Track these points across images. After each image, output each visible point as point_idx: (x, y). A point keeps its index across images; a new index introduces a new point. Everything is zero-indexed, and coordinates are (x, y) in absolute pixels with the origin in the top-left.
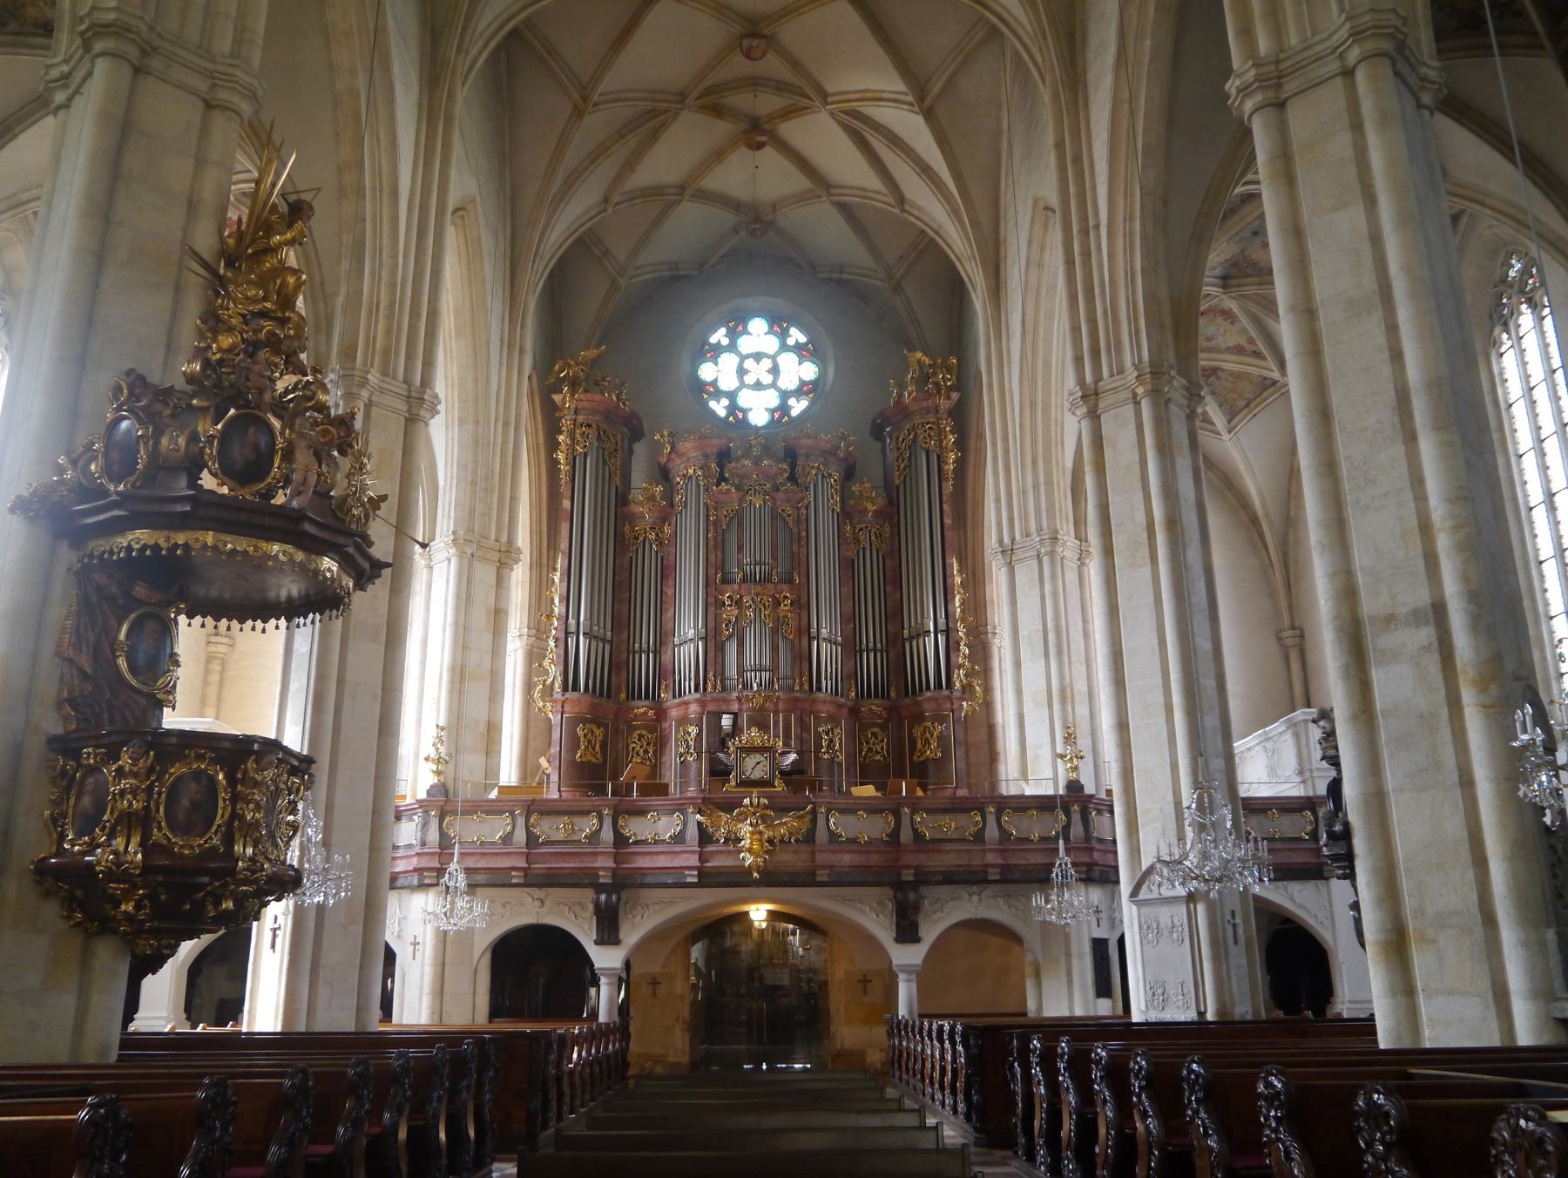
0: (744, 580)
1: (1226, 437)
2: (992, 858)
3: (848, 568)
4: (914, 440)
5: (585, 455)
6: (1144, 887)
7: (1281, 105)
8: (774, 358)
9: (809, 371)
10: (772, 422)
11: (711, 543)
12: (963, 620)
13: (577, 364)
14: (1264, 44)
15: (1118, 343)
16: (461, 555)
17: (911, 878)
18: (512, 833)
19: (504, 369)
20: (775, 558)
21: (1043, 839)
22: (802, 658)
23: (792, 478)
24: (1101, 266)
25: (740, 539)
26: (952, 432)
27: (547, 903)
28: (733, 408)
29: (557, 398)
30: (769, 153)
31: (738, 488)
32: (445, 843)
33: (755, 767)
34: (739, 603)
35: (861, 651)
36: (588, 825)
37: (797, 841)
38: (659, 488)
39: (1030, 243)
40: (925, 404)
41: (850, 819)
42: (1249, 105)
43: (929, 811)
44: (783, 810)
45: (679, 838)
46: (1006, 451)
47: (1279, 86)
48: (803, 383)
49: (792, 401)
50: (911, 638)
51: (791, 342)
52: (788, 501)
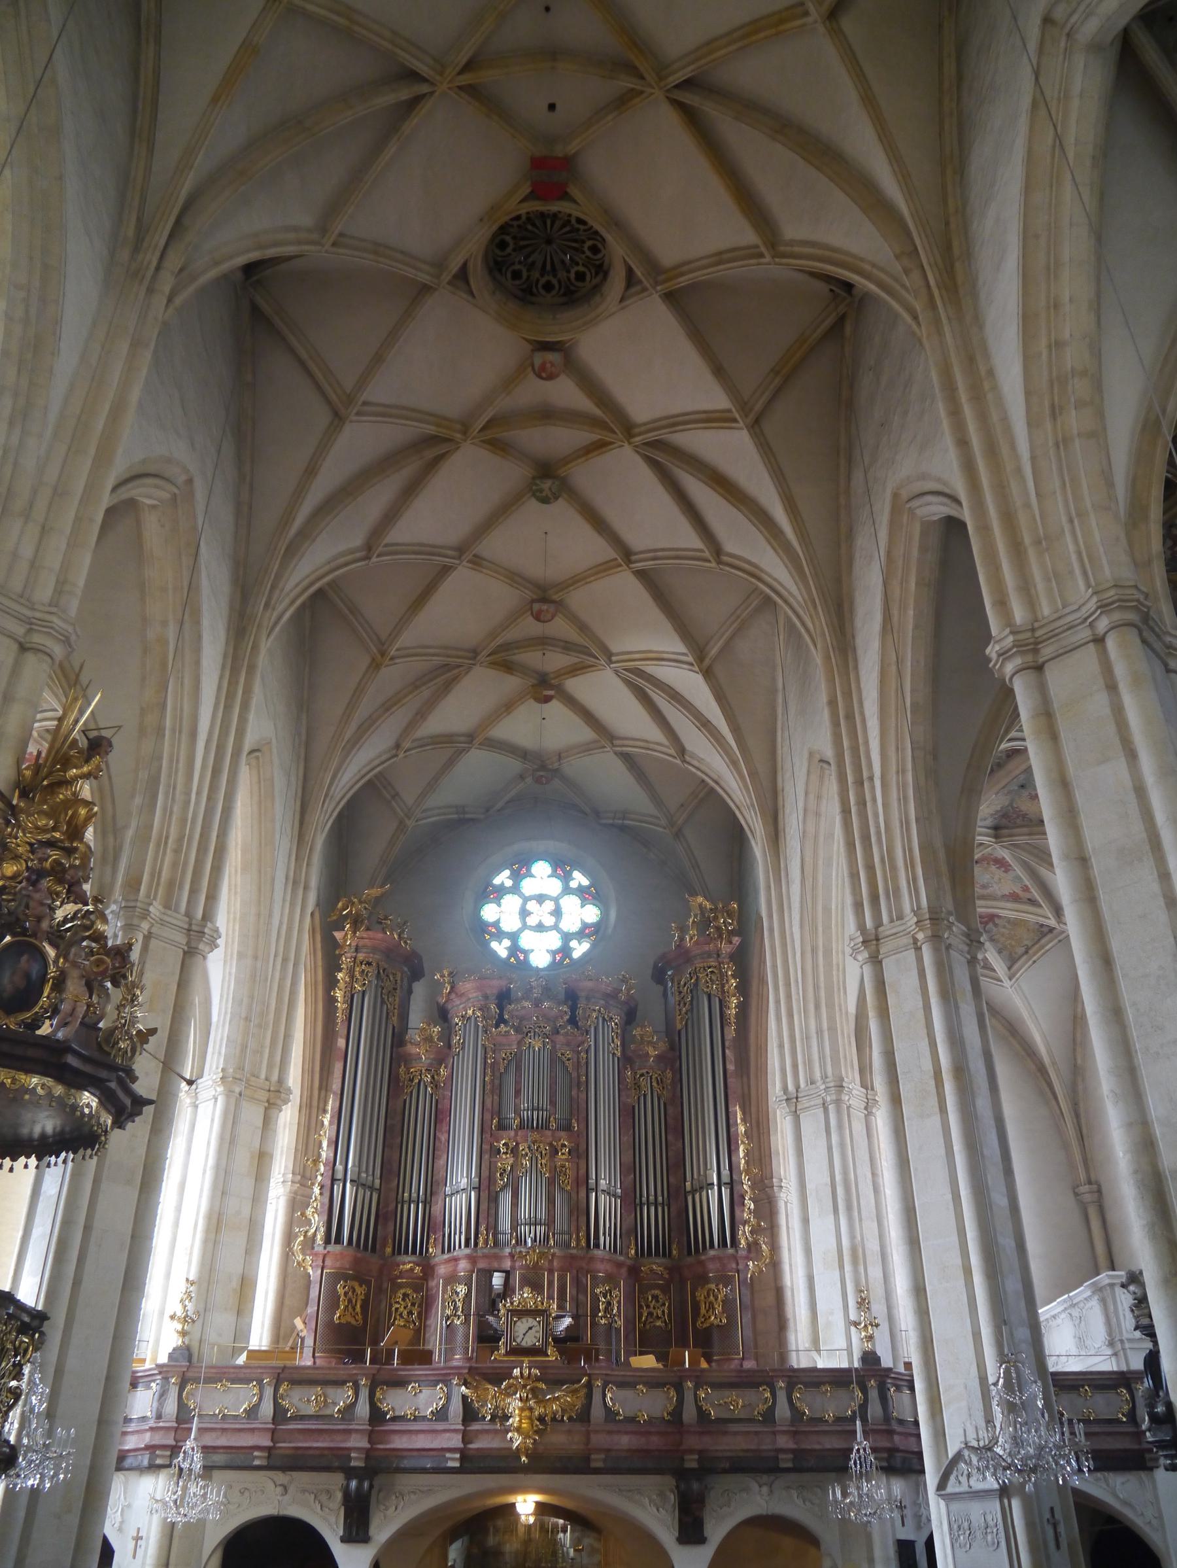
0: (521, 1127)
1: (1007, 983)
2: (783, 1442)
3: (628, 1115)
4: (696, 984)
5: (364, 993)
6: (952, 1478)
7: (1039, 668)
8: (556, 900)
9: (592, 914)
10: (554, 965)
11: (488, 1087)
12: (747, 1172)
13: (360, 902)
14: (1019, 615)
15: (897, 890)
16: (229, 1093)
17: (694, 1465)
18: (257, 1405)
19: (287, 905)
20: (553, 1103)
21: (839, 1420)
22: (580, 1212)
23: (573, 1021)
24: (876, 815)
25: (518, 1083)
26: (733, 976)
27: (291, 1490)
28: (515, 949)
29: (338, 935)
30: (556, 706)
31: (518, 1030)
32: (183, 1416)
33: (527, 1332)
34: (514, 1151)
35: (641, 1204)
36: (342, 1397)
37: (570, 1419)
38: (437, 1029)
39: (806, 794)
40: (706, 948)
41: (628, 1393)
42: (1009, 668)
43: (714, 1386)
44: (555, 1383)
45: (441, 1414)
46: (789, 997)
47: (1036, 651)
48: (585, 926)
49: (574, 944)
50: (693, 1191)
51: (573, 884)
52: (568, 1044)
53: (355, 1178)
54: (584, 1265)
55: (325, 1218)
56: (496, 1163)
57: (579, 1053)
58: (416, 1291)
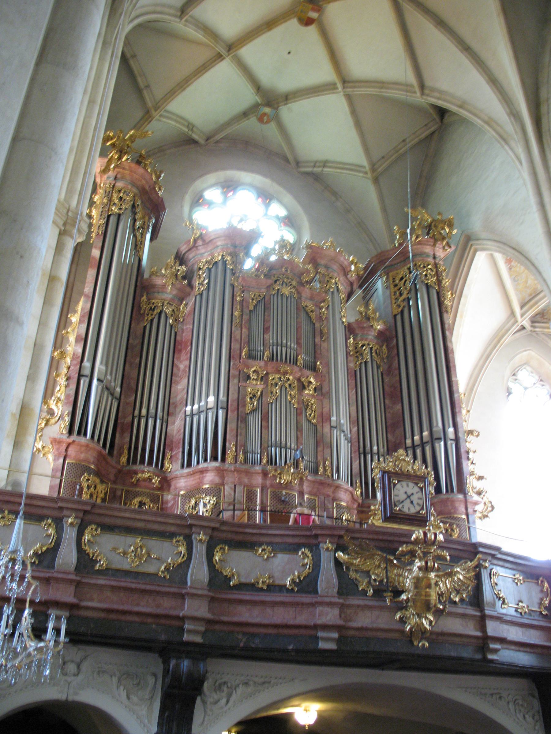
18: (54, 550)
34: (264, 379)
37: (462, 600)
45: (307, 585)
52: (311, 299)
53: (102, 378)
54: (330, 493)
55: (71, 409)
56: (245, 388)
57: (321, 308)
58: (152, 501)
